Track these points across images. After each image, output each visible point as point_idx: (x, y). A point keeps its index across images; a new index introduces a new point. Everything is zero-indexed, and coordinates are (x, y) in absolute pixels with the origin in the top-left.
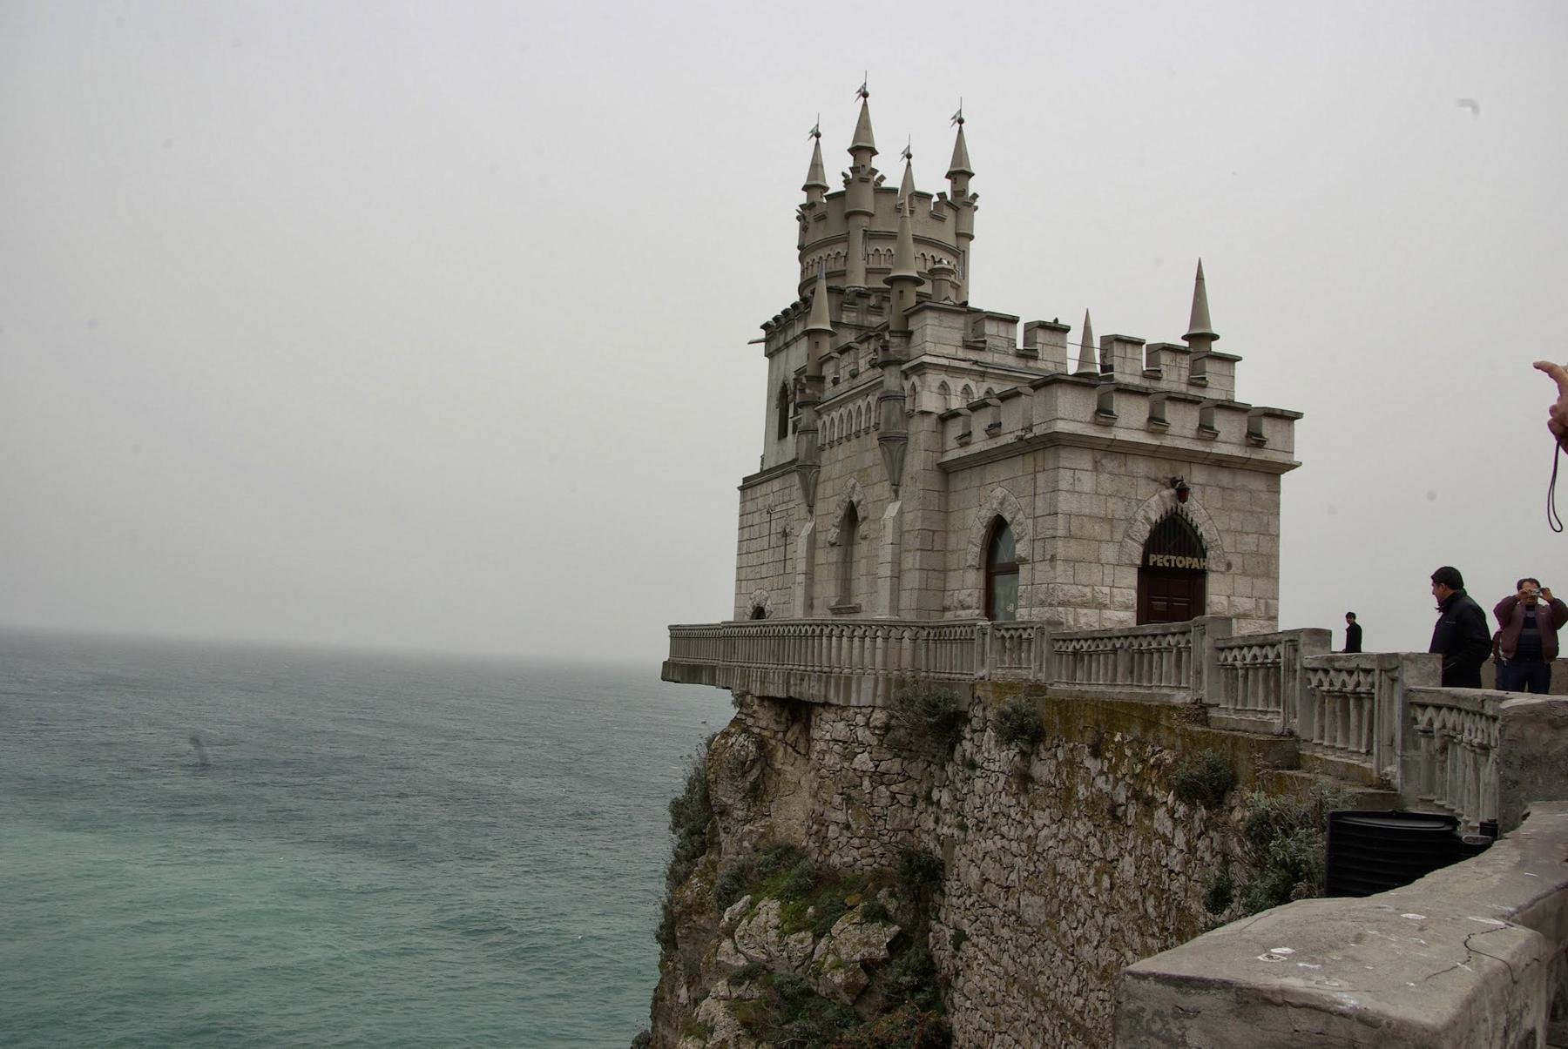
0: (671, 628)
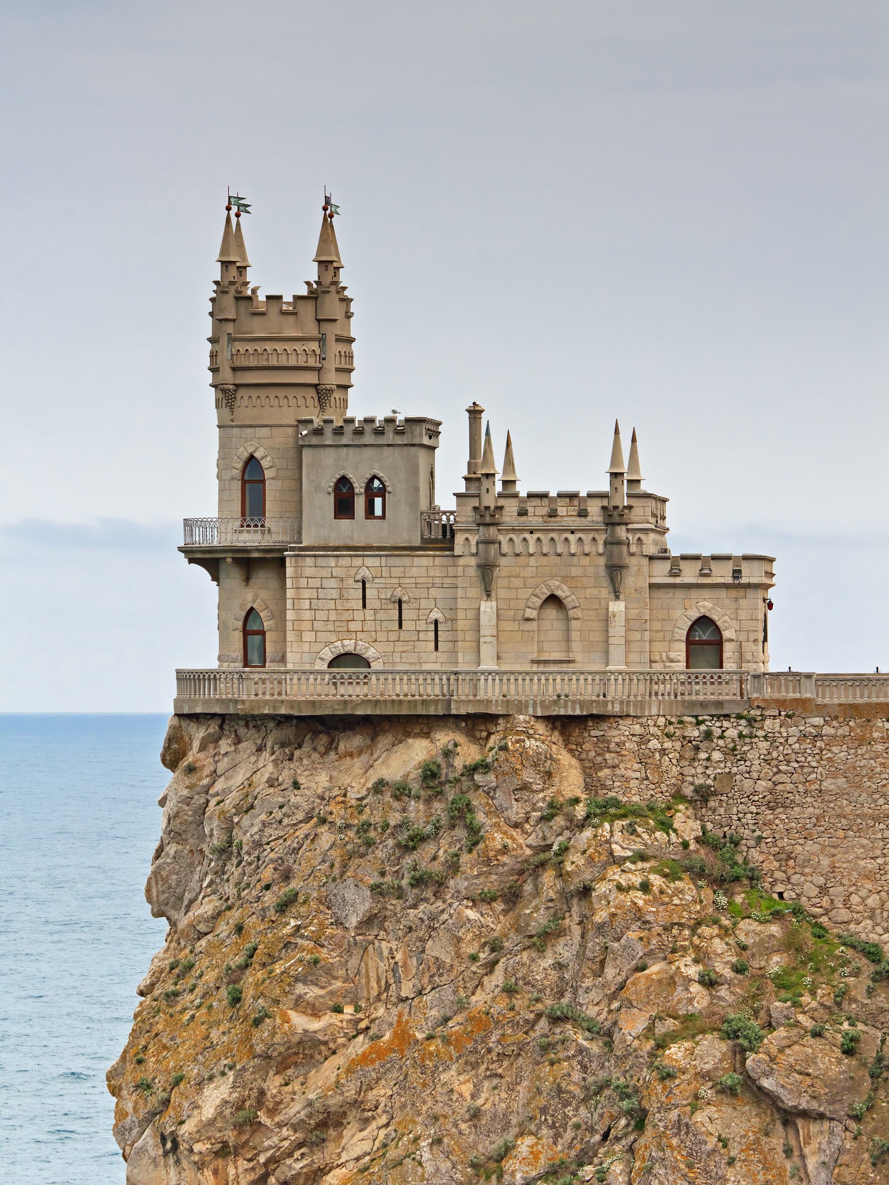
0: (178, 672)
